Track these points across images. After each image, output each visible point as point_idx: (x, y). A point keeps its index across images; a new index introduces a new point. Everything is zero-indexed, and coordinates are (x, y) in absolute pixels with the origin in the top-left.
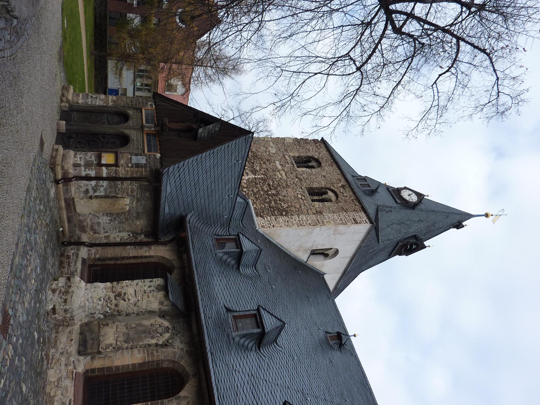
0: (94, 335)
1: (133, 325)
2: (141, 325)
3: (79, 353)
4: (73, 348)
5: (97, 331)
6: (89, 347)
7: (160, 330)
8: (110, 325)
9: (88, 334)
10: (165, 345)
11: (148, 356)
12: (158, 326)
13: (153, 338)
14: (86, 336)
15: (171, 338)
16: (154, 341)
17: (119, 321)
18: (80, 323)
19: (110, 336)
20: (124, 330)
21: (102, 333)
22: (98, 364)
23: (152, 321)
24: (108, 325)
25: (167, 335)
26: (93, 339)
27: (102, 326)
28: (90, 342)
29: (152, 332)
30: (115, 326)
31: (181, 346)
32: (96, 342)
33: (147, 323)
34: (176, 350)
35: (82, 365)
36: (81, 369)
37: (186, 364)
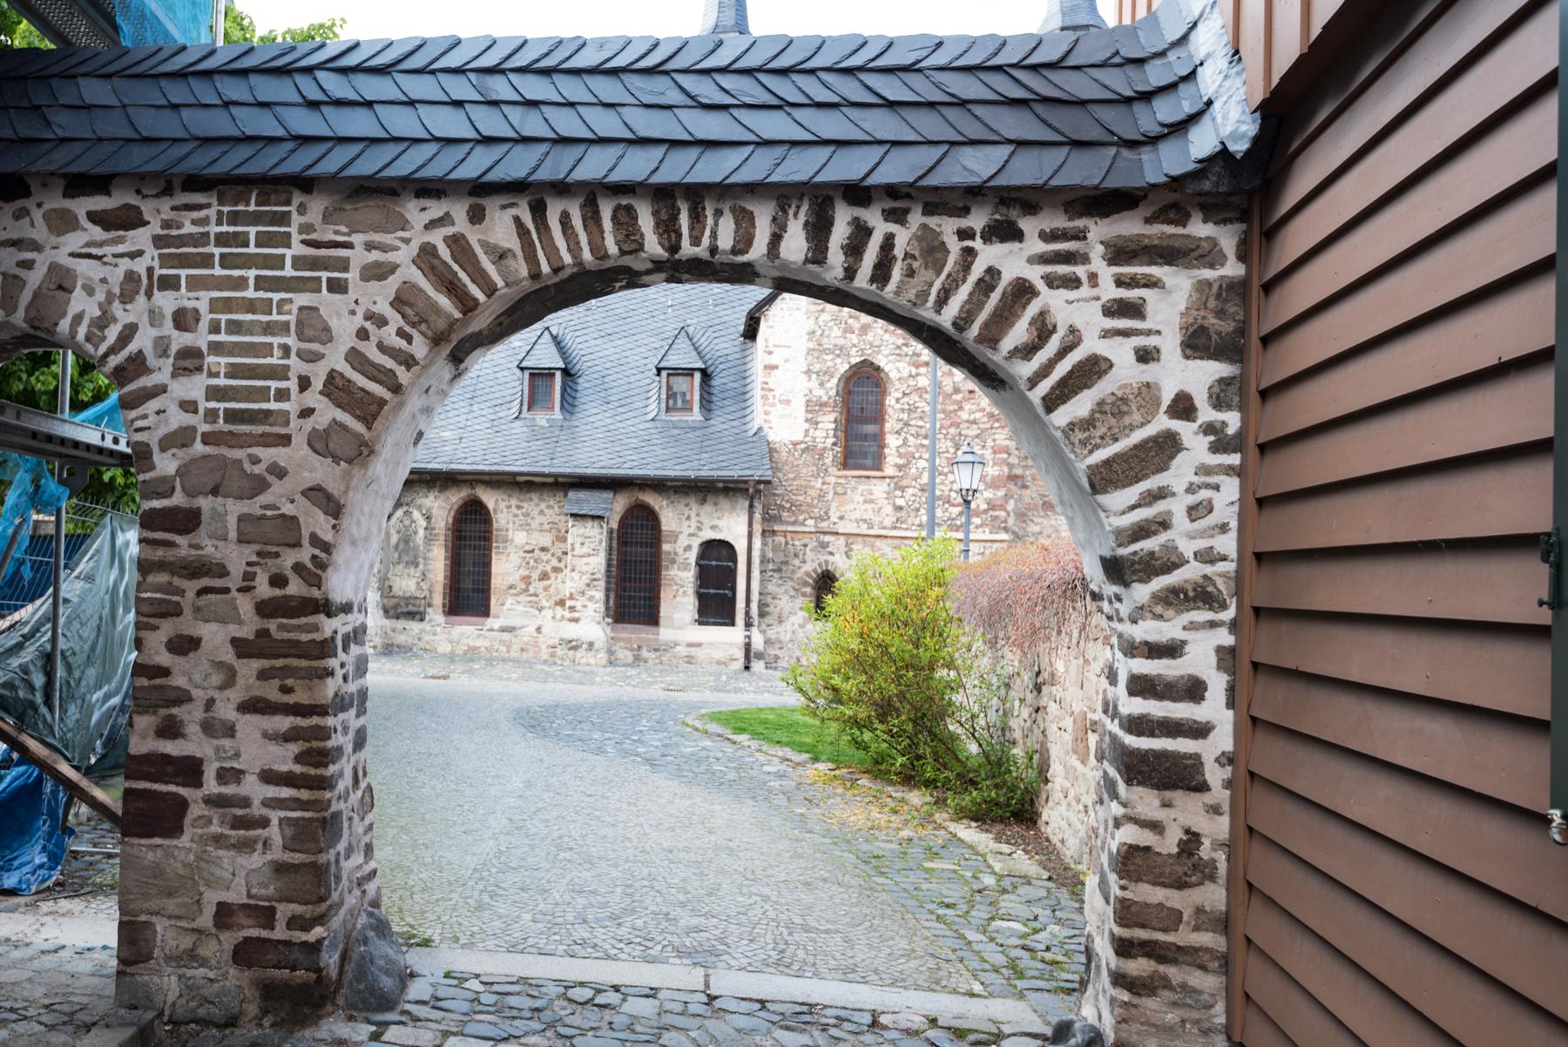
2: (397, 546)
3: (422, 620)
4: (414, 626)
7: (407, 523)
10: (428, 518)
13: (416, 533)
15: (419, 508)
16: (421, 532)
19: (406, 584)
22: (438, 599)
23: (393, 531)
25: (416, 514)
28: (411, 608)
31: (431, 497)
33: (394, 538)
35: (436, 616)
36: (441, 619)
37: (456, 497)
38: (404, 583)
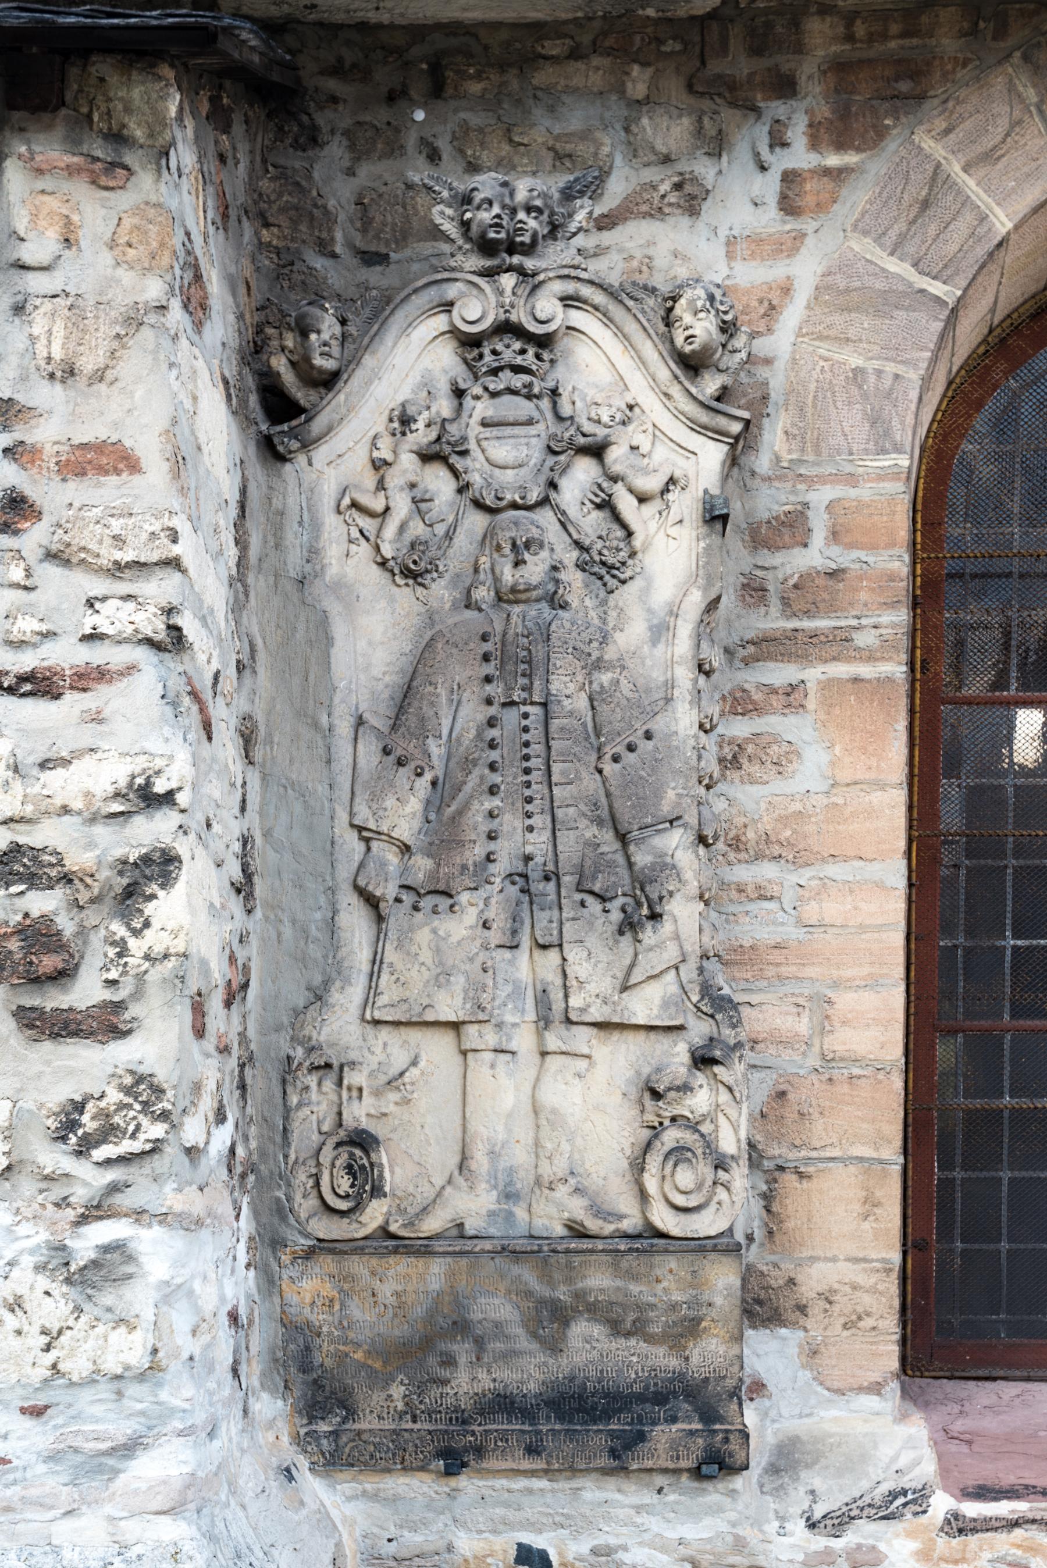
0: (496, 1308)
1: (404, 814)
2: (407, 698)
5: (435, 1273)
6: (663, 1359)
8: (359, 1114)
9: (467, 1382)
11: (840, 644)
12: (439, 483)
14: (503, 1404)
17: (319, 996)
18: (313, 1486)
20: (459, 927)
21: (474, 1206)
24: (362, 1141)
26: (551, 1319)
27: (375, 1214)
28: (590, 1349)
29: (535, 569)
30: (391, 1049)
32: (599, 1280)
33: (373, 634)
34: (806, 270)
38: (502, 1093)
